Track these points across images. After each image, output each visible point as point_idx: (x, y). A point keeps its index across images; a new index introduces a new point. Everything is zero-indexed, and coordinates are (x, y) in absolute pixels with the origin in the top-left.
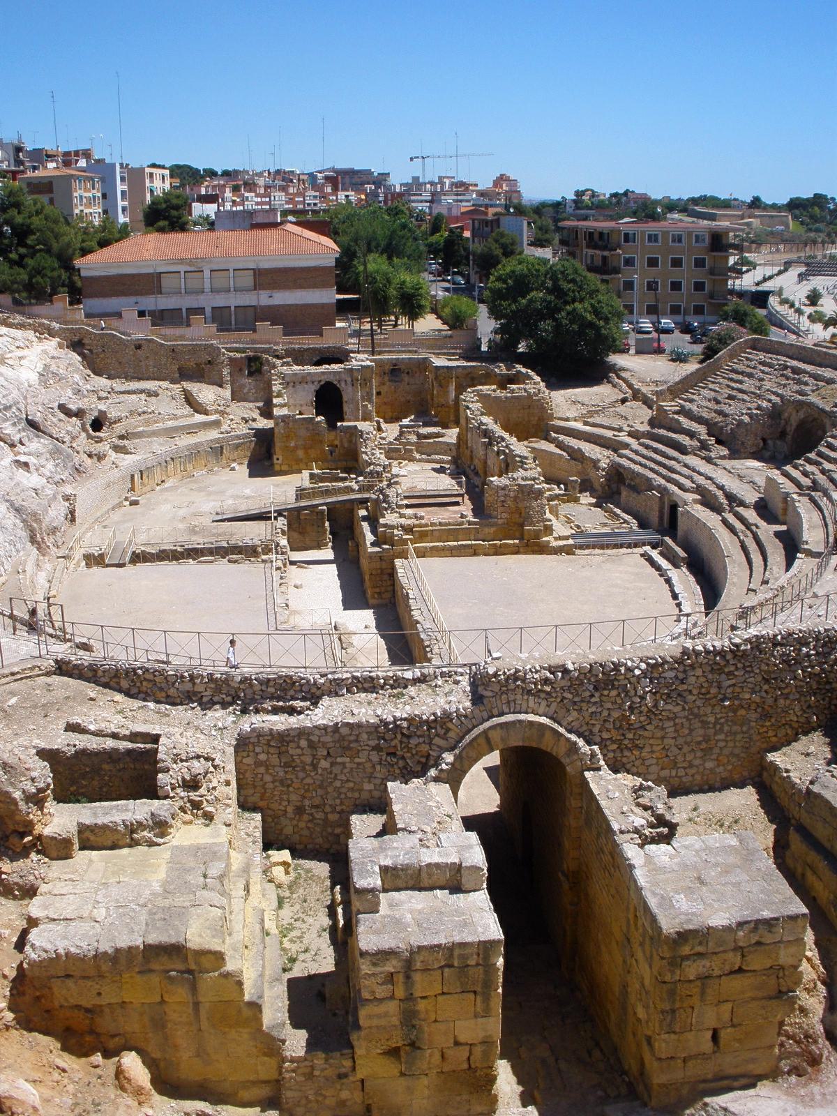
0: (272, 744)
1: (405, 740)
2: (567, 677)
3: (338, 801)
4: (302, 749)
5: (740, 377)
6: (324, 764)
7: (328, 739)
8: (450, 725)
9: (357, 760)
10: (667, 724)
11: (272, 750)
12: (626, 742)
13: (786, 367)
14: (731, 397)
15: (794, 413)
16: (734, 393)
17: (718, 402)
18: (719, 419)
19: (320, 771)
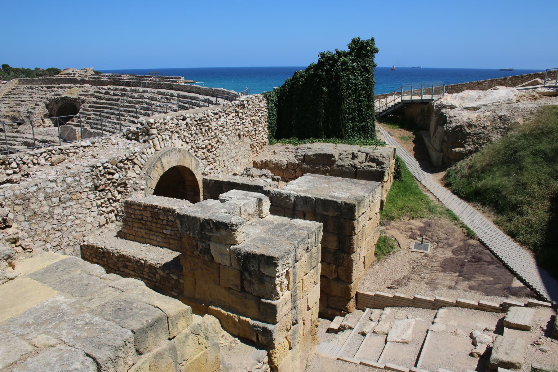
0: (16, 202)
1: (110, 177)
2: (185, 122)
3: (71, 238)
4: (41, 202)
5: (17, 96)
6: (58, 210)
7: (60, 189)
8: (135, 161)
9: (80, 201)
10: (223, 147)
11: (18, 208)
12: (211, 159)
13: (42, 87)
14: (18, 104)
15: (55, 105)
16: (18, 102)
17: (11, 107)
18: (16, 113)
19: (55, 217)
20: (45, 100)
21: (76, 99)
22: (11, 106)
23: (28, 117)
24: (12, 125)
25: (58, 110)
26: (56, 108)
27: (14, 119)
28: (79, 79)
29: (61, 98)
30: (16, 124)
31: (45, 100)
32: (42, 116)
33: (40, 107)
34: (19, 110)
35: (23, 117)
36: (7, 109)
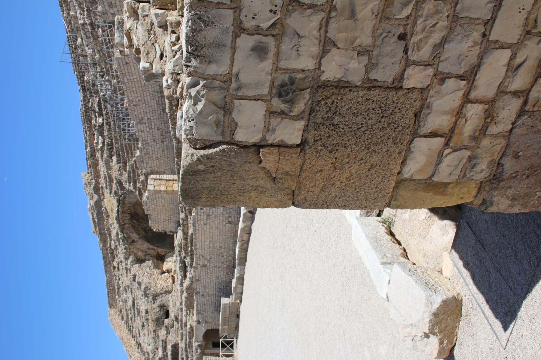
14: (139, 312)
17: (143, 326)
20: (129, 262)
21: (119, 201)
22: (141, 324)
23: (155, 297)
24: (167, 327)
25: (148, 241)
26: (143, 245)
27: (159, 322)
28: (96, 197)
29: (122, 232)
30: (166, 321)
31: (129, 262)
32: (156, 272)
33: (139, 273)
34: (144, 311)
35: (155, 306)
36: (146, 331)
